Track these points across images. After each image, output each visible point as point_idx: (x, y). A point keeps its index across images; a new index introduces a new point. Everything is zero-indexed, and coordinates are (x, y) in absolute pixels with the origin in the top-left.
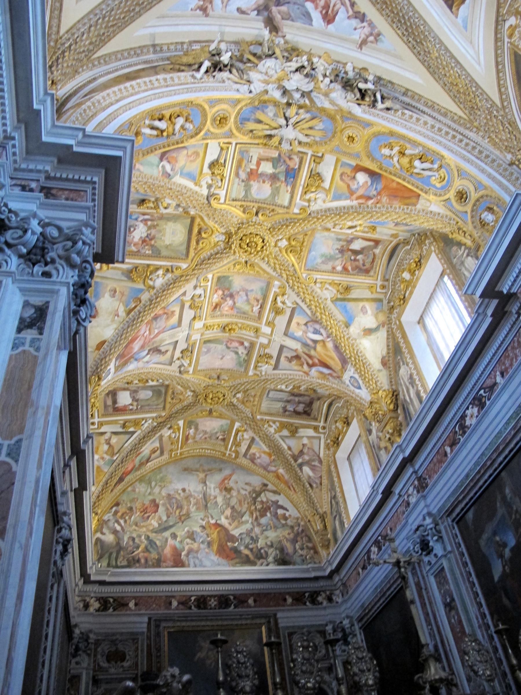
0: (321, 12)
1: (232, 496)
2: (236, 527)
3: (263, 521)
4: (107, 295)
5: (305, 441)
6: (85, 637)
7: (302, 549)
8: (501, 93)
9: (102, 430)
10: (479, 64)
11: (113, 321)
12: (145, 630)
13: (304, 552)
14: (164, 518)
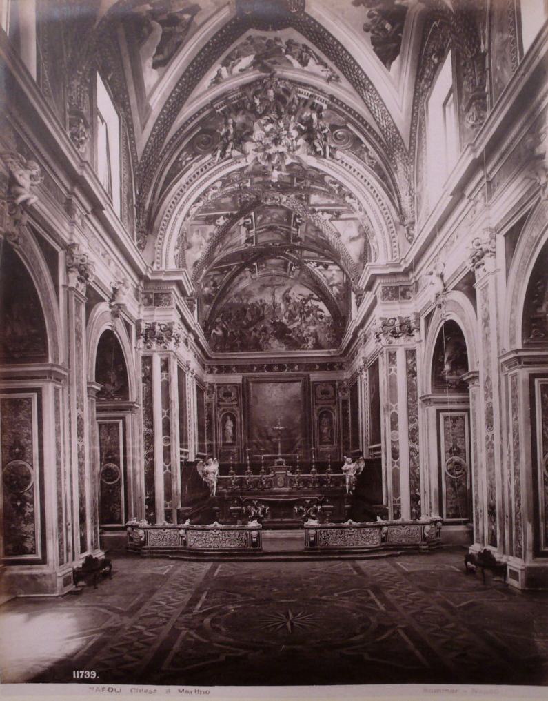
0: (298, 60)
3: (308, 319)
4: (194, 234)
5: (334, 272)
6: (212, 385)
8: (411, 138)
10: (401, 111)
11: (200, 248)
12: (241, 382)
14: (250, 319)
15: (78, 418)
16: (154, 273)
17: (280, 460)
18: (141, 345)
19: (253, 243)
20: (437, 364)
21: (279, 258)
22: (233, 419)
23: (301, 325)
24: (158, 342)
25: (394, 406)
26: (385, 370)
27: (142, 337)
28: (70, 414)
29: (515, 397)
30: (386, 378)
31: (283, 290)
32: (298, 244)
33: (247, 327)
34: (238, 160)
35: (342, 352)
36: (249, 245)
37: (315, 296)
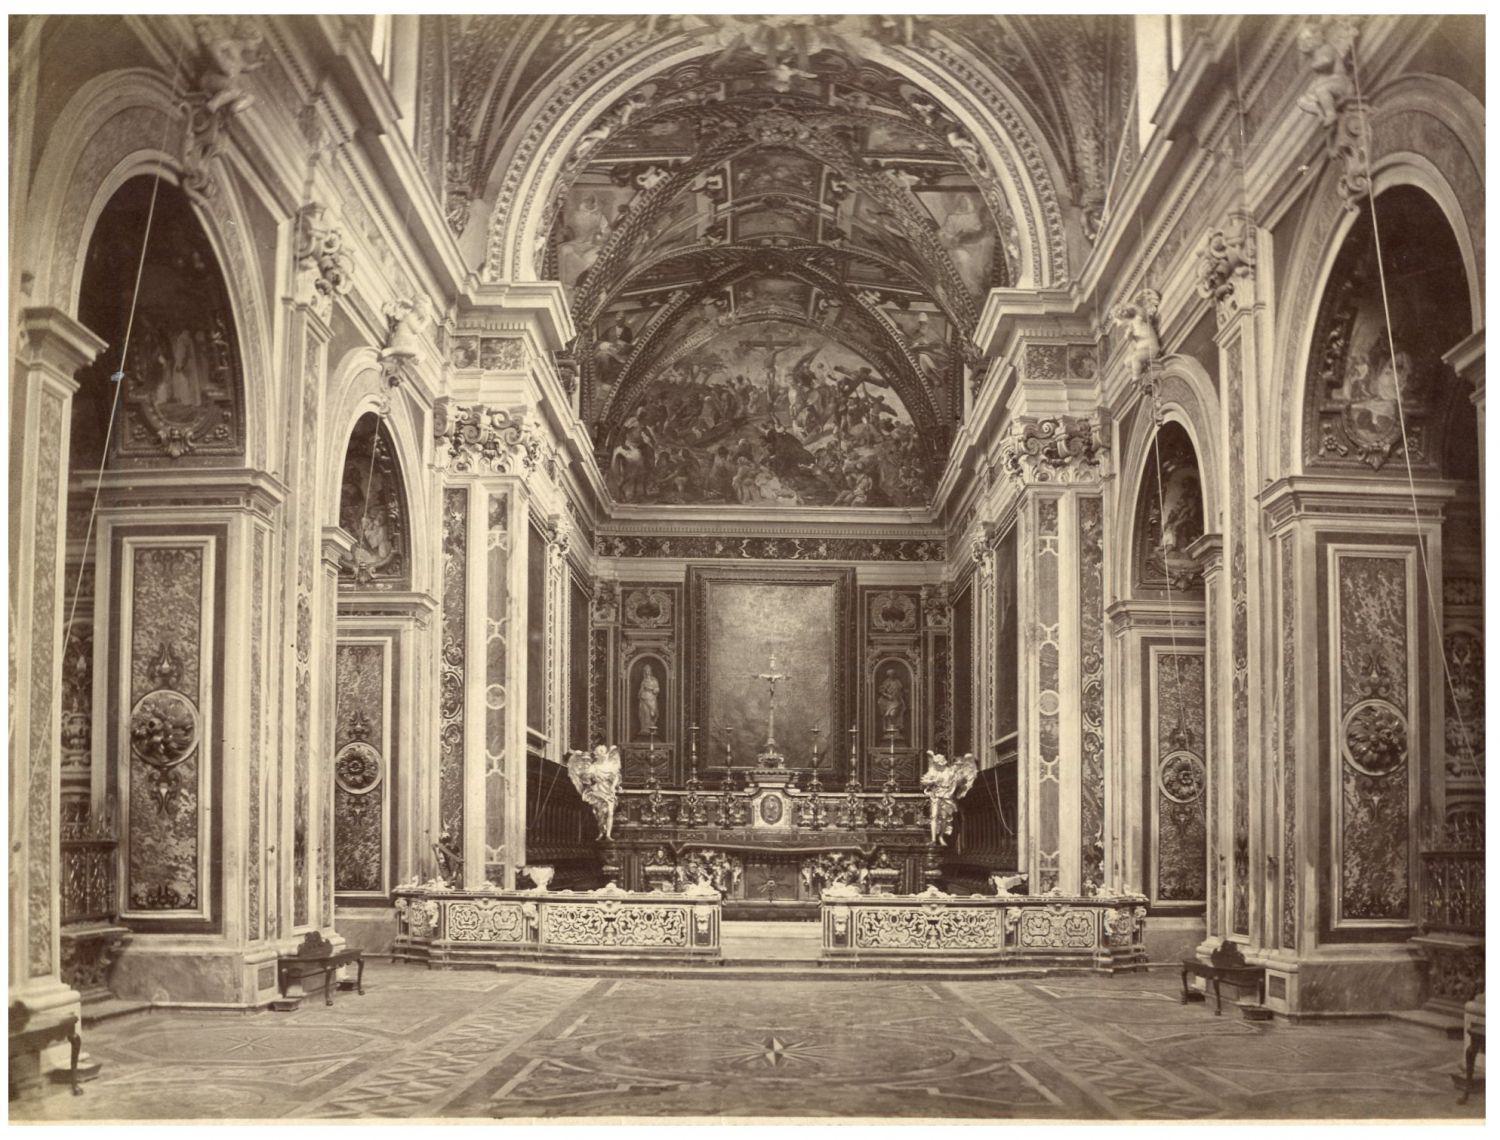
1: (812, 389)
2: (815, 439)
3: (855, 430)
5: (924, 318)
6: (609, 586)
7: (907, 476)
9: (613, 309)
11: (595, 242)
12: (682, 580)
13: (909, 482)
14: (711, 424)
15: (300, 606)
16: (482, 290)
17: (772, 755)
18: (444, 460)
19: (724, 237)
20: (1146, 530)
21: (790, 278)
22: (659, 673)
23: (837, 444)
24: (485, 455)
25: (1049, 630)
26: (1030, 542)
27: (446, 440)
28: (283, 593)
29: (1289, 584)
30: (1031, 562)
31: (798, 354)
32: (835, 243)
33: (702, 444)
34: (699, 39)
35: (936, 516)
36: (715, 241)
37: (875, 374)
